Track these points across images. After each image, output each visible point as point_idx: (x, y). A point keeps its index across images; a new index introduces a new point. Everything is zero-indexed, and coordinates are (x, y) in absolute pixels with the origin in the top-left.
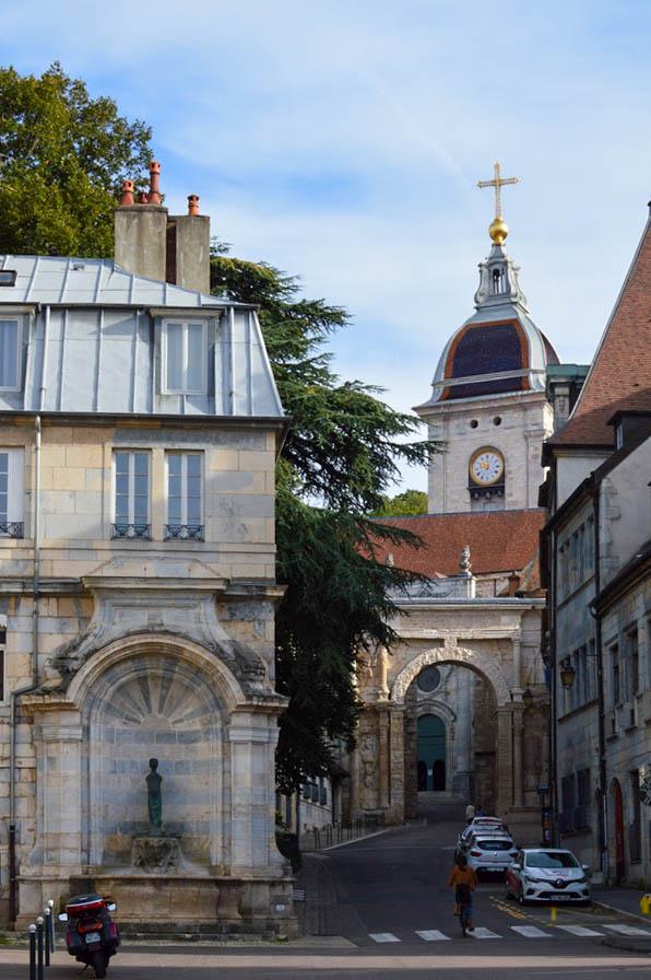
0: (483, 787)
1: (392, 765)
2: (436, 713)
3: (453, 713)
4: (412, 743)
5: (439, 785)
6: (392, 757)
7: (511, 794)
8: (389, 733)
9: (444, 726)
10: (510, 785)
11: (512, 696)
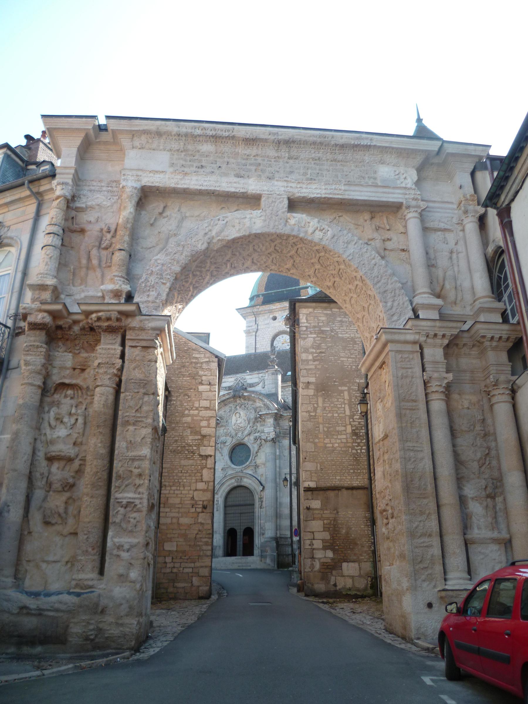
0: (318, 544)
1: (116, 464)
3: (262, 485)
4: (205, 472)
5: (248, 550)
6: (120, 445)
7: (436, 551)
8: (119, 384)
10: (433, 524)
11: (414, 311)
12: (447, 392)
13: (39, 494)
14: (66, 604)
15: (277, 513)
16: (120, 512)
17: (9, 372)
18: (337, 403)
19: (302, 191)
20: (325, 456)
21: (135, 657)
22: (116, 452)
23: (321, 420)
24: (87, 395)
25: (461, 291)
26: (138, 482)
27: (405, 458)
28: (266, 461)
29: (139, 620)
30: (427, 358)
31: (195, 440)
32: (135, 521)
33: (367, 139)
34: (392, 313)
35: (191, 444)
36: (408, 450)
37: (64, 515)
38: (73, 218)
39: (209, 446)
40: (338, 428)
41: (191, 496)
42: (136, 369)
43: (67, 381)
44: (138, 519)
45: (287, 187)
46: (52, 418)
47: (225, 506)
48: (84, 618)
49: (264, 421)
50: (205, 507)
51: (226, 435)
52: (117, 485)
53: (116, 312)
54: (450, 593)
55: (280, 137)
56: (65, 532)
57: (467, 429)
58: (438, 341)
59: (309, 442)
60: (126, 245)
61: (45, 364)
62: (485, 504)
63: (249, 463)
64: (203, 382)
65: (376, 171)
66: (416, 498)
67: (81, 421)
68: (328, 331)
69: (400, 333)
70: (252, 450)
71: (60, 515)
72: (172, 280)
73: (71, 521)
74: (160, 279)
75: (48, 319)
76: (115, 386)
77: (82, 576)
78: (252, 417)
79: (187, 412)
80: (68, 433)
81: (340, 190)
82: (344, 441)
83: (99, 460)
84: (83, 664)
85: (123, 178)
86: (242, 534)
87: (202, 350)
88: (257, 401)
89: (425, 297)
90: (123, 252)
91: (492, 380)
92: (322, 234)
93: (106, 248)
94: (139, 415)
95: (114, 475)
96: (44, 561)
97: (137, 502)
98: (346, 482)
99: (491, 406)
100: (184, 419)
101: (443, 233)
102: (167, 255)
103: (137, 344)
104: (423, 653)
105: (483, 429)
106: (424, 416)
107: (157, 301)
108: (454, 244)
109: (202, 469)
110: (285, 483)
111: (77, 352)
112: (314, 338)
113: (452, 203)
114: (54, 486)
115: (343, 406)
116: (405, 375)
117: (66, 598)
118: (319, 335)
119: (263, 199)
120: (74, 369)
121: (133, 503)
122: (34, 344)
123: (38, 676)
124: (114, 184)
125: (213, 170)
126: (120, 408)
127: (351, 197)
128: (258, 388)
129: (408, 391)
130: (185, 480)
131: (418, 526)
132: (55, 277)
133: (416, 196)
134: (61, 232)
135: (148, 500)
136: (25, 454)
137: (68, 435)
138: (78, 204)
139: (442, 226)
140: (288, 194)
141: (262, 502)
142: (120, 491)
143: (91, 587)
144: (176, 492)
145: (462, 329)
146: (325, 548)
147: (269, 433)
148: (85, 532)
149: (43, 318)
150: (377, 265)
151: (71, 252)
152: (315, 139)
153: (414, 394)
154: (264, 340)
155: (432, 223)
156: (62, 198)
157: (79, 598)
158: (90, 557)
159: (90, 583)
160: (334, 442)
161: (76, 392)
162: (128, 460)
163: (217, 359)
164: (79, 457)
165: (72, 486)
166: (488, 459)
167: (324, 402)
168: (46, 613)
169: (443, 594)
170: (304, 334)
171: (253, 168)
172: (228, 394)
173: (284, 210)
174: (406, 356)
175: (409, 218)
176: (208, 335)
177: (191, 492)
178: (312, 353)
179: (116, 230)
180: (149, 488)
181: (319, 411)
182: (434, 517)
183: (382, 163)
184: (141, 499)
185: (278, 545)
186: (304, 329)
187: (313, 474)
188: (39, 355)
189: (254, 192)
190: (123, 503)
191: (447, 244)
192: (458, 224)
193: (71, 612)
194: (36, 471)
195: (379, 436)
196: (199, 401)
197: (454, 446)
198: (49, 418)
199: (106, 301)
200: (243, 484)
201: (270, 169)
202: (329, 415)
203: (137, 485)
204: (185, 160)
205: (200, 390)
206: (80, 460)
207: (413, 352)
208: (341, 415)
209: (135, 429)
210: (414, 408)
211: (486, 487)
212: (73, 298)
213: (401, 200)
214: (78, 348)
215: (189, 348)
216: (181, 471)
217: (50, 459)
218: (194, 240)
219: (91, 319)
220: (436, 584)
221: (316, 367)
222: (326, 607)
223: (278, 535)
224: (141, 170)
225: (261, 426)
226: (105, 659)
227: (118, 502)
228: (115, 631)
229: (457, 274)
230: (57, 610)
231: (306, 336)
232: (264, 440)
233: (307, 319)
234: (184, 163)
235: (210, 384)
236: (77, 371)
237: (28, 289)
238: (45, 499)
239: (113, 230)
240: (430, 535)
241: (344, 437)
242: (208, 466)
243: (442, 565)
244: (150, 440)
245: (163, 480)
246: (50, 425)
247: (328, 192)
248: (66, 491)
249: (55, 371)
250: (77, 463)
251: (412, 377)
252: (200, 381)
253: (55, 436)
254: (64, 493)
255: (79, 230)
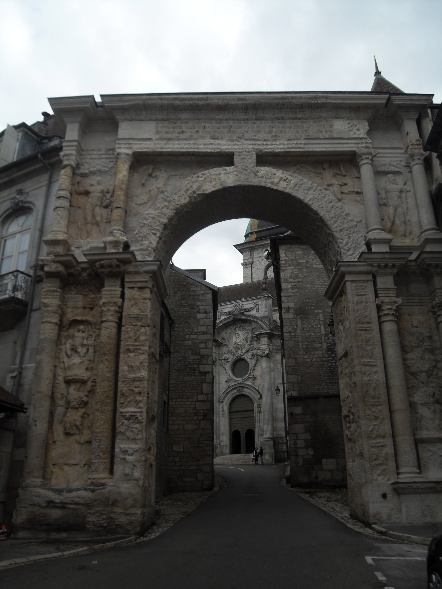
0: (301, 444)
1: (121, 385)
2: (247, 394)
3: (259, 393)
6: (123, 368)
7: (389, 450)
8: (120, 319)
9: (253, 403)
10: (386, 428)
11: (368, 245)
12: (397, 314)
13: (60, 410)
14: (83, 498)
15: (273, 417)
16: (124, 424)
17: (33, 313)
18: (313, 324)
19: (268, 147)
20: (304, 369)
21: (139, 540)
22: (120, 375)
23: (300, 339)
24: (96, 328)
25: (410, 225)
26: (139, 398)
27: (361, 372)
28: (262, 373)
29: (142, 511)
30: (379, 286)
31: (196, 359)
32: (137, 430)
33: (323, 97)
34: (348, 248)
35: (192, 363)
36: (364, 365)
37: (80, 427)
38: (78, 183)
39: (207, 364)
40: (315, 345)
41: (194, 406)
42: (134, 306)
43: (79, 318)
44: (140, 429)
45: (255, 144)
46: (68, 349)
47: (230, 413)
48: (98, 510)
49: (259, 339)
50: (205, 415)
51: (229, 352)
52: (121, 401)
53: (115, 260)
54: (402, 485)
55: (247, 102)
56: (82, 441)
57: (416, 345)
58: (388, 271)
59: (291, 358)
60: (122, 203)
61: (60, 305)
62: (433, 408)
63: (249, 376)
64: (200, 311)
65: (332, 125)
66: (371, 405)
67: (91, 350)
68: (304, 263)
69: (354, 265)
70: (250, 364)
71: (77, 427)
72: (161, 231)
73: (86, 432)
74: (151, 230)
75: (61, 268)
76: (117, 320)
77: (96, 476)
78: (249, 336)
79: (187, 337)
80: (82, 361)
81: (301, 144)
82: (321, 356)
83: (106, 382)
84: (96, 547)
85: (117, 146)
86: (244, 435)
87: (199, 284)
88: (253, 323)
89: (376, 233)
90: (119, 209)
91: (437, 302)
92: (285, 183)
93: (106, 207)
94: (137, 344)
95: (119, 394)
96: (66, 464)
97: (138, 415)
98: (323, 391)
99: (438, 324)
100: (186, 342)
101: (392, 175)
102: (155, 210)
103: (134, 286)
104: (377, 536)
105: (430, 344)
106: (377, 336)
107: (149, 249)
108: (403, 184)
109: (202, 383)
110: (278, 392)
111: (86, 294)
112: (292, 269)
113: (400, 148)
114: (72, 404)
115: (319, 326)
116: (360, 301)
117: (83, 493)
118: (296, 267)
119: (235, 157)
120: (85, 308)
121: (135, 416)
122: (51, 289)
123: (59, 556)
124: (111, 152)
125: (192, 135)
126: (122, 338)
127: (310, 150)
128: (253, 313)
129: (363, 315)
130: (188, 393)
131: (373, 429)
132: (66, 233)
133: (367, 145)
134: (69, 195)
135: (147, 412)
136: (47, 379)
137: (81, 362)
138: (82, 171)
139: (392, 169)
140: (255, 150)
141: (260, 408)
142: (124, 407)
143: (103, 484)
144: (181, 403)
145: (409, 259)
146: (306, 447)
147: (263, 350)
148: (97, 441)
149: (57, 268)
150: (334, 207)
151: (78, 211)
152: (277, 101)
153: (368, 317)
154: (259, 271)
155: (383, 167)
156: (69, 167)
157: (93, 494)
158: (102, 460)
159: (102, 481)
160: (312, 357)
161: (86, 327)
162: (129, 381)
163: (211, 291)
164: (91, 380)
165: (86, 404)
166: (435, 370)
167: (302, 323)
168: (68, 506)
169: (396, 486)
170: (284, 267)
171: (226, 130)
172: (229, 318)
173: (253, 165)
174: (361, 284)
175: (362, 165)
176: (204, 271)
177: (193, 403)
178: (291, 282)
179: (114, 191)
180: (148, 403)
181: (298, 331)
182: (387, 421)
183: (337, 118)
184: (141, 412)
185: (275, 444)
186: (284, 262)
187: (295, 385)
188: (55, 298)
189: (227, 151)
190: (127, 416)
191: (397, 184)
192: (406, 166)
193: (88, 505)
194: (58, 392)
195: (341, 353)
196: (198, 326)
197: (404, 360)
198: (66, 349)
199: (107, 251)
200: (243, 393)
201: (240, 130)
202: (307, 334)
203: (138, 401)
204: (169, 128)
205: (198, 318)
206: (92, 382)
207: (367, 281)
208: (318, 334)
209: (135, 355)
210: (368, 329)
211: (434, 394)
212: (81, 249)
213: (354, 149)
214: (87, 290)
215: (188, 283)
216: (185, 385)
217: (68, 382)
218: (178, 195)
219: (96, 266)
220: (389, 477)
221: (294, 294)
222: (306, 497)
223: (275, 435)
224: (132, 139)
225: (257, 344)
226: (114, 543)
227: (123, 416)
228: (123, 520)
229: (405, 210)
230: (77, 504)
231: (285, 268)
232: (260, 355)
233: (285, 254)
234: (167, 130)
235: (206, 313)
236: (87, 310)
237: (44, 245)
238: (65, 415)
239: (111, 191)
240: (384, 437)
241: (321, 352)
242: (207, 381)
243: (394, 461)
244: (147, 364)
245: (170, 394)
246: (67, 355)
247: (290, 146)
248: (81, 408)
249: (69, 310)
250: (90, 384)
251: (367, 303)
252: (198, 310)
253: (71, 364)
254: (80, 409)
255: (84, 192)
